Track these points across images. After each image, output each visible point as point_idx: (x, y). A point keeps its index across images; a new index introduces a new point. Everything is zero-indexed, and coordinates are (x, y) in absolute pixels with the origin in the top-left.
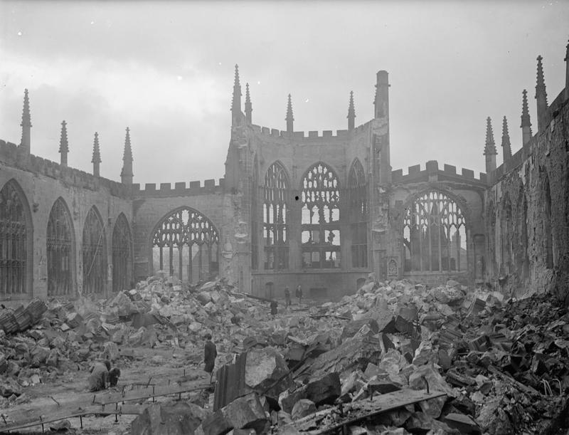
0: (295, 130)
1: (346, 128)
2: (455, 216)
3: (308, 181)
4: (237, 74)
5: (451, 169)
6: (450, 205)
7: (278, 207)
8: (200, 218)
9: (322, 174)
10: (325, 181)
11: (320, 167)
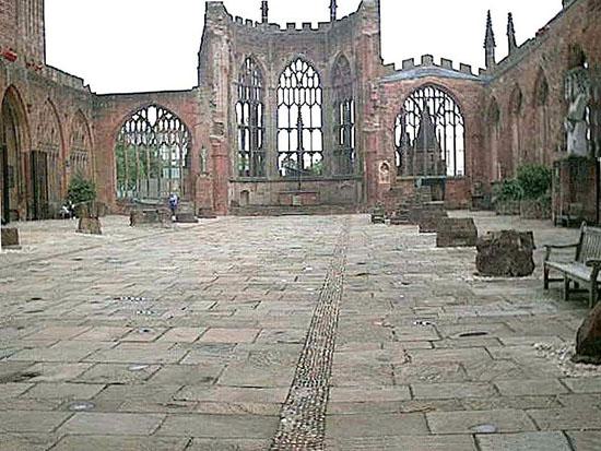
5: (446, 62)
8: (169, 116)
10: (305, 78)
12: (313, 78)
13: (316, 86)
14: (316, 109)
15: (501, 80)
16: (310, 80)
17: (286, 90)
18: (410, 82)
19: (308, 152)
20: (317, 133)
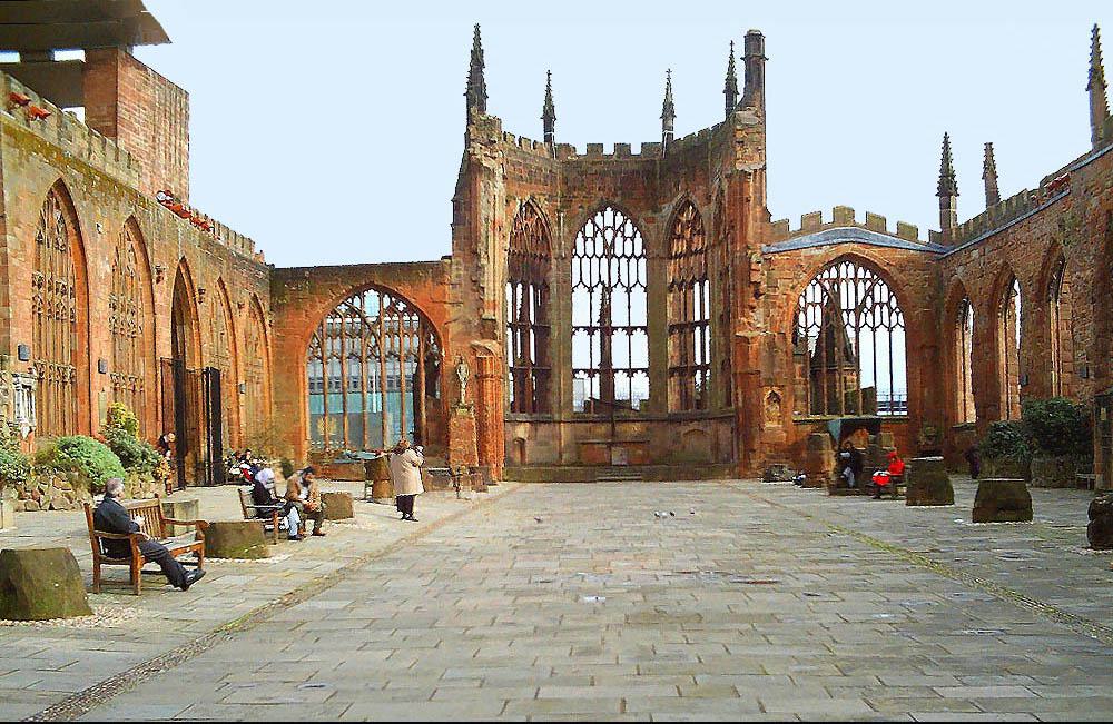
0: (560, 137)
1: (656, 136)
2: (885, 307)
3: (586, 239)
5: (875, 223)
6: (877, 288)
7: (520, 286)
9: (613, 228)
10: (619, 240)
11: (609, 212)
12: (632, 239)
13: (638, 253)
14: (639, 296)
15: (975, 254)
17: (585, 260)
18: (817, 252)
19: (625, 370)
20: (640, 339)
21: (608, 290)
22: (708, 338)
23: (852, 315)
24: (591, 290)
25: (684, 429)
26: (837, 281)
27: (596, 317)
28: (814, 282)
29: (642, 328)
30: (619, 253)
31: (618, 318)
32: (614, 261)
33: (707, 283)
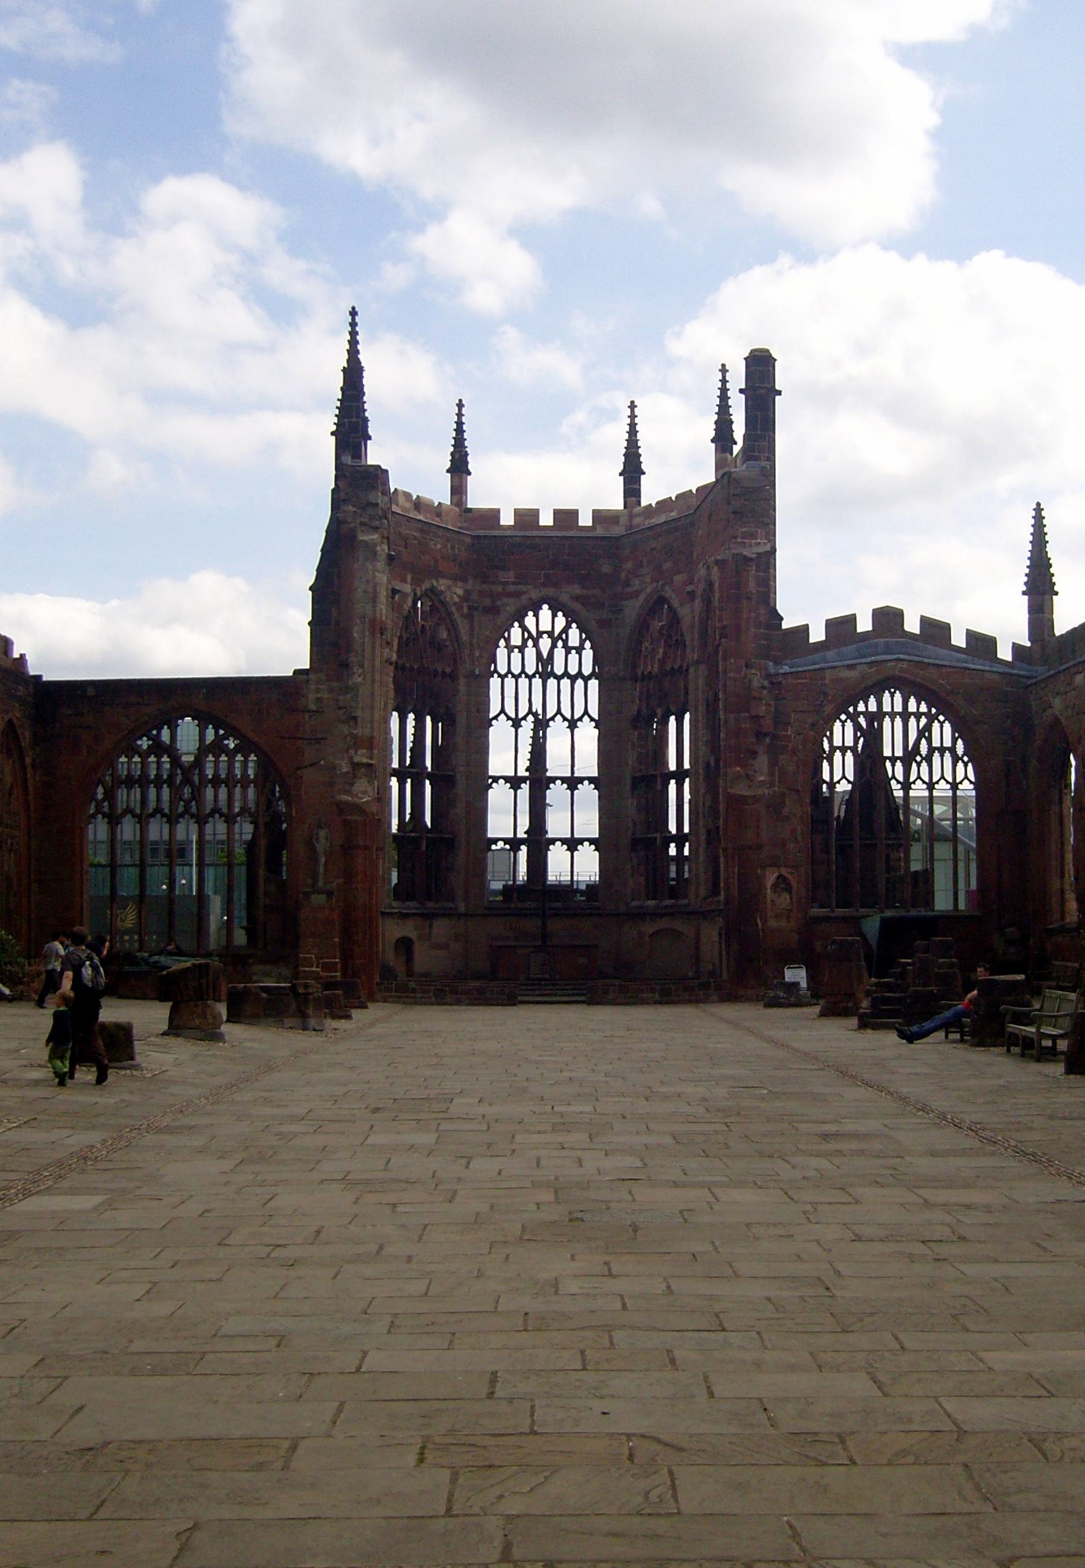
0: (476, 499)
1: (615, 502)
2: (947, 754)
3: (510, 649)
4: (353, 334)
6: (936, 725)
7: (411, 716)
9: (550, 634)
10: (559, 653)
11: (545, 612)
14: (588, 736)
16: (573, 656)
17: (510, 682)
19: (564, 841)
20: (588, 794)
21: (541, 725)
22: (687, 796)
23: (899, 764)
24: (516, 723)
25: (649, 928)
26: (880, 715)
27: (524, 763)
28: (843, 717)
29: (591, 780)
30: (559, 670)
31: (556, 764)
32: (552, 683)
33: (687, 716)
